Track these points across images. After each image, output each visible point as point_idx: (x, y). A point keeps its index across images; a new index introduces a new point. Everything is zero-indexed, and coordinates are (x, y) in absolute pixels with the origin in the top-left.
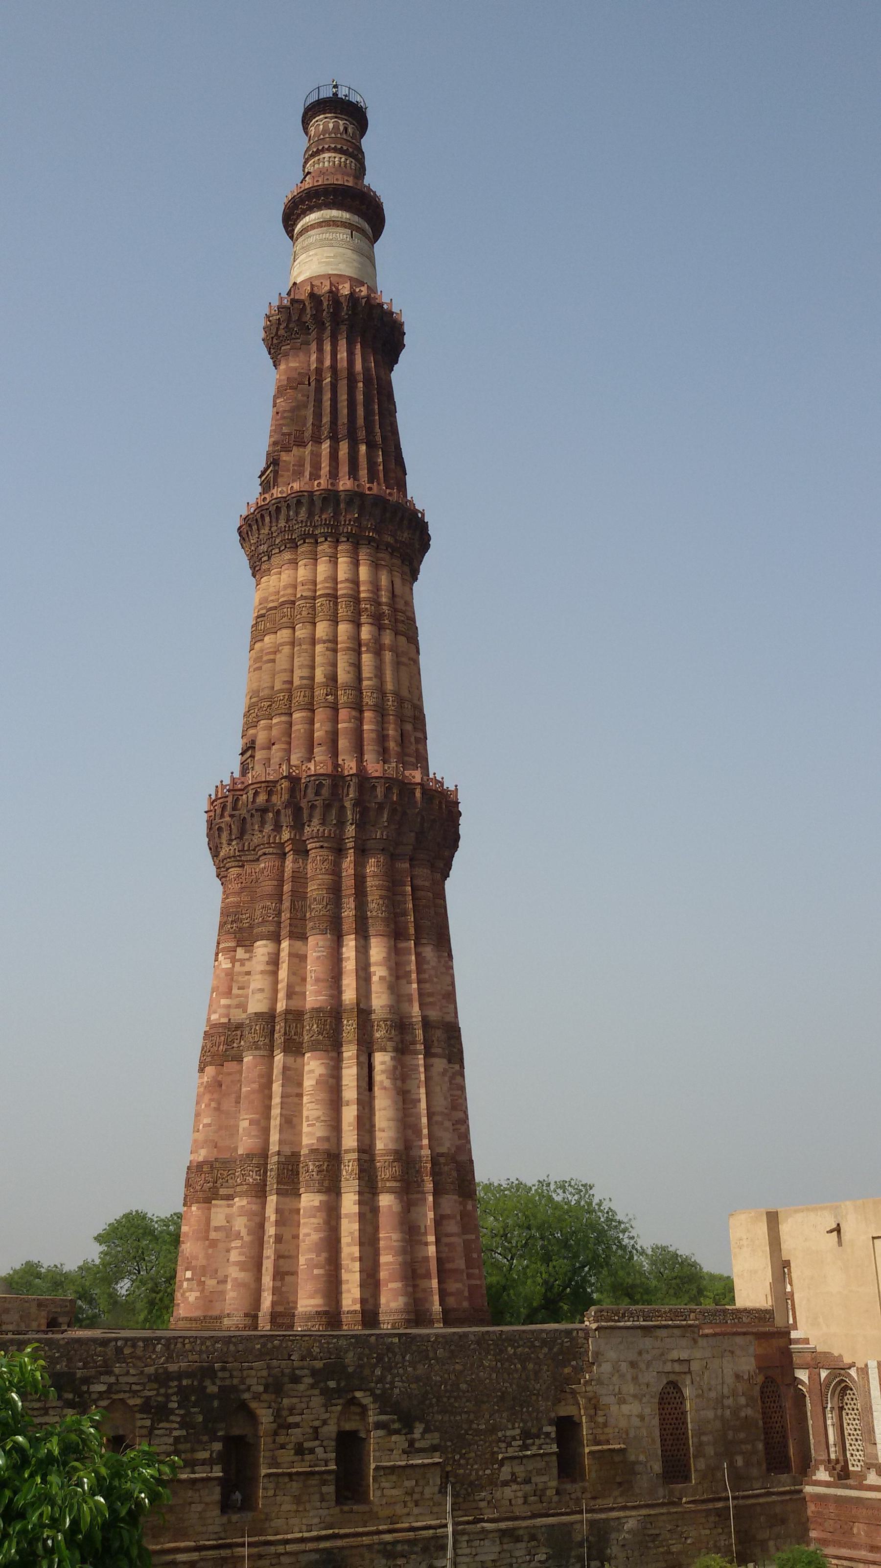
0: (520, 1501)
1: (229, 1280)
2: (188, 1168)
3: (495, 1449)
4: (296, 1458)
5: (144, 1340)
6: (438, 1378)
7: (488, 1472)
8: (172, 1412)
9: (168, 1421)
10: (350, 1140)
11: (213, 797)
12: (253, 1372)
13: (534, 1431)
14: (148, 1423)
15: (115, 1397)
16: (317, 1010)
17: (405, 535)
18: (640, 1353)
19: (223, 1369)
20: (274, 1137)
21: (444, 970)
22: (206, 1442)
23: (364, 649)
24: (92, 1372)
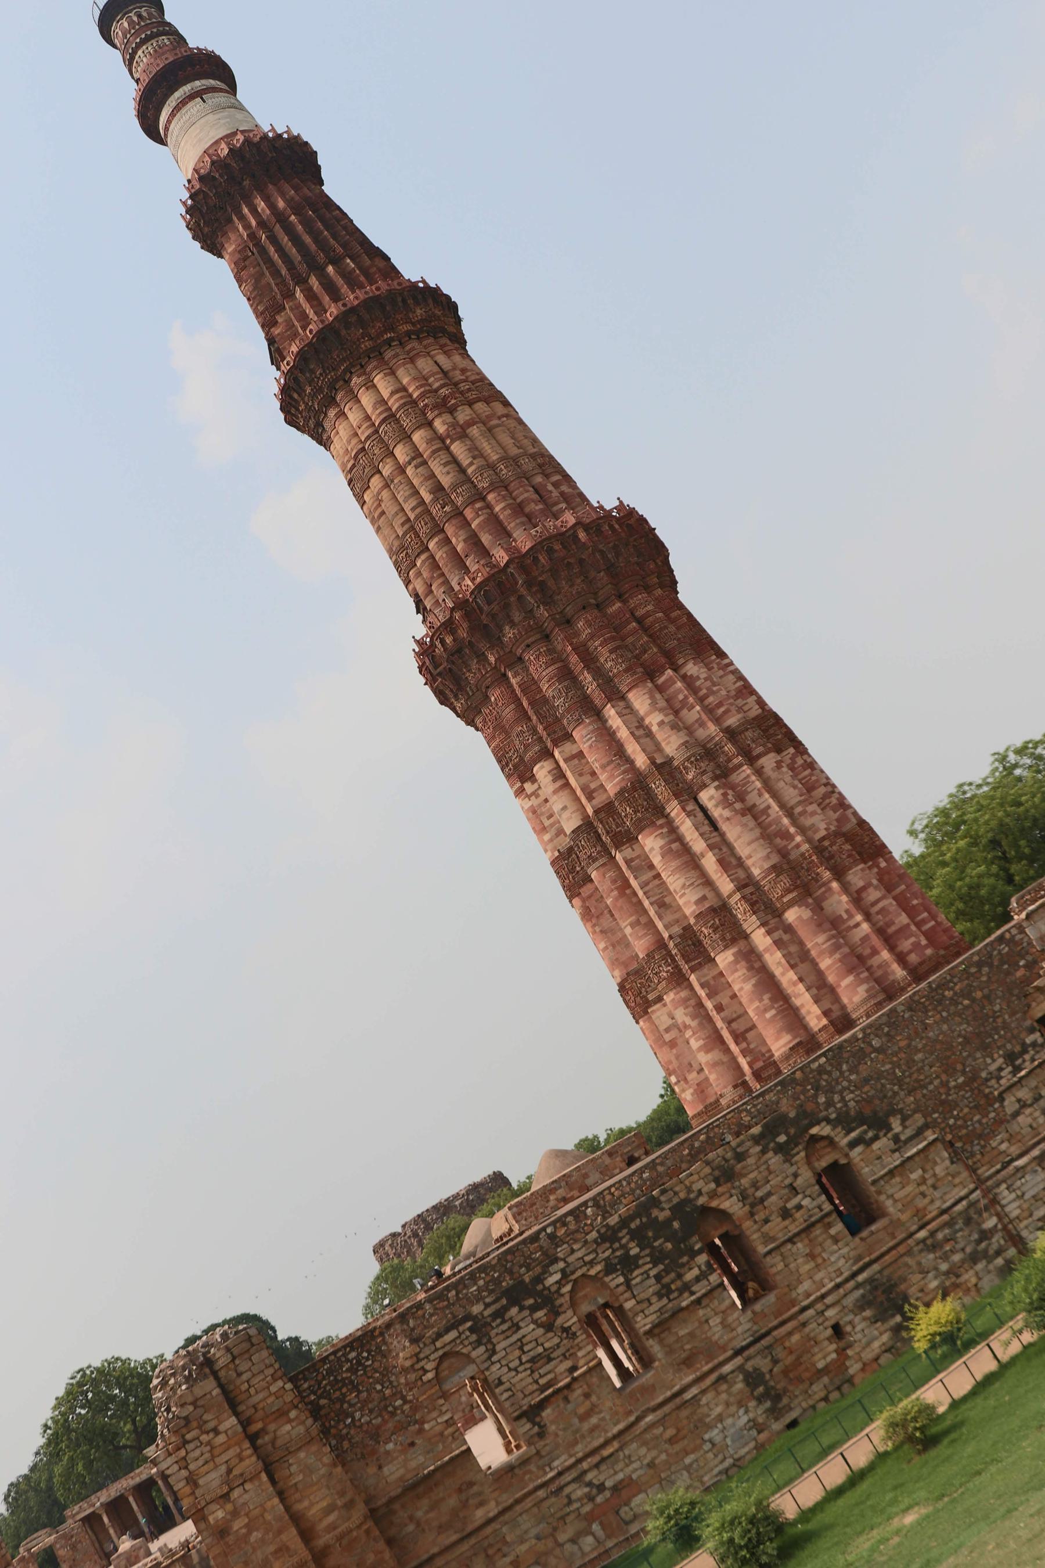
3: (987, 1091)
4: (787, 1222)
6: (888, 1067)
7: (992, 1115)
8: (637, 1257)
9: (638, 1267)
10: (726, 885)
12: (695, 1177)
13: (1018, 1049)
14: (621, 1279)
15: (573, 1277)
16: (620, 793)
17: (419, 312)
19: (663, 1192)
20: (660, 925)
22: (688, 1262)
24: (538, 1270)
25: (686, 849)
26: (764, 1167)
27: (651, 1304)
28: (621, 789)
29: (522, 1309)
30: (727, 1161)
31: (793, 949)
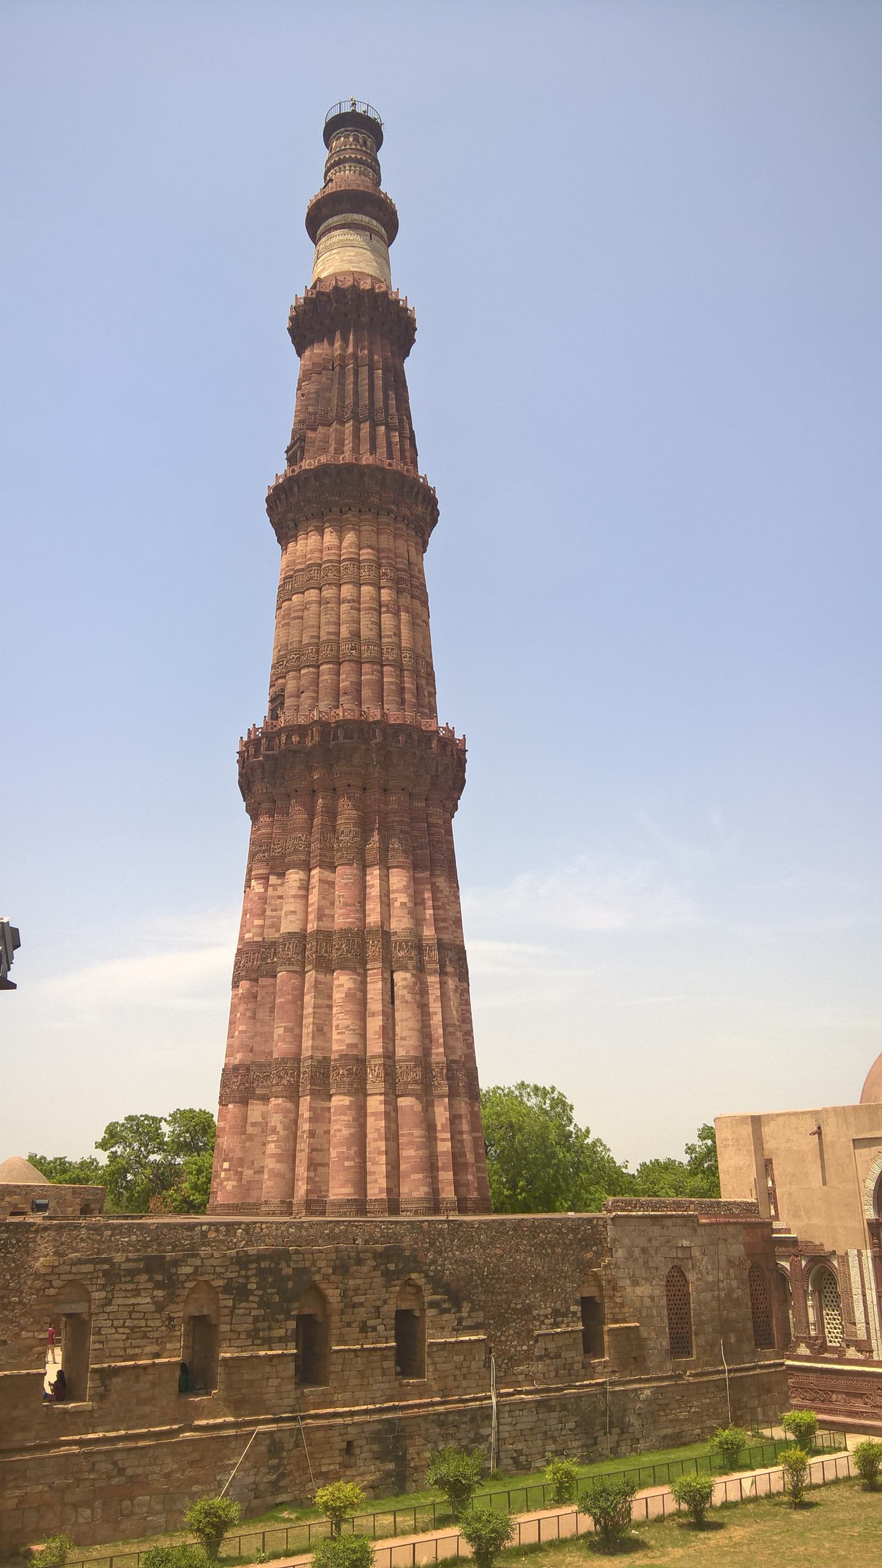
0: (552, 1374)
1: (266, 1170)
2: (223, 1070)
3: (531, 1327)
5: (227, 1224)
7: (525, 1348)
8: (251, 1292)
9: (247, 1301)
10: (375, 1047)
11: (245, 739)
12: (323, 1255)
13: (563, 1310)
14: (230, 1303)
18: (650, 1240)
20: (307, 1043)
21: (453, 899)
23: (383, 609)
25: (364, 1003)
26: (370, 1281)
27: (239, 1338)
28: (348, 929)
29: (150, 1280)
30: (349, 1258)
31: (393, 1126)
